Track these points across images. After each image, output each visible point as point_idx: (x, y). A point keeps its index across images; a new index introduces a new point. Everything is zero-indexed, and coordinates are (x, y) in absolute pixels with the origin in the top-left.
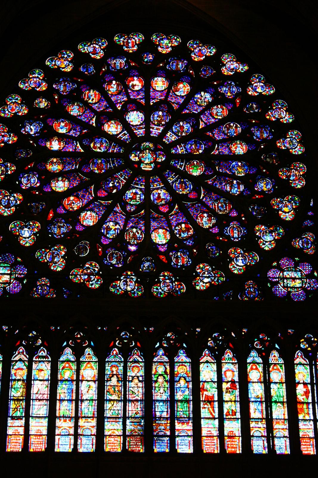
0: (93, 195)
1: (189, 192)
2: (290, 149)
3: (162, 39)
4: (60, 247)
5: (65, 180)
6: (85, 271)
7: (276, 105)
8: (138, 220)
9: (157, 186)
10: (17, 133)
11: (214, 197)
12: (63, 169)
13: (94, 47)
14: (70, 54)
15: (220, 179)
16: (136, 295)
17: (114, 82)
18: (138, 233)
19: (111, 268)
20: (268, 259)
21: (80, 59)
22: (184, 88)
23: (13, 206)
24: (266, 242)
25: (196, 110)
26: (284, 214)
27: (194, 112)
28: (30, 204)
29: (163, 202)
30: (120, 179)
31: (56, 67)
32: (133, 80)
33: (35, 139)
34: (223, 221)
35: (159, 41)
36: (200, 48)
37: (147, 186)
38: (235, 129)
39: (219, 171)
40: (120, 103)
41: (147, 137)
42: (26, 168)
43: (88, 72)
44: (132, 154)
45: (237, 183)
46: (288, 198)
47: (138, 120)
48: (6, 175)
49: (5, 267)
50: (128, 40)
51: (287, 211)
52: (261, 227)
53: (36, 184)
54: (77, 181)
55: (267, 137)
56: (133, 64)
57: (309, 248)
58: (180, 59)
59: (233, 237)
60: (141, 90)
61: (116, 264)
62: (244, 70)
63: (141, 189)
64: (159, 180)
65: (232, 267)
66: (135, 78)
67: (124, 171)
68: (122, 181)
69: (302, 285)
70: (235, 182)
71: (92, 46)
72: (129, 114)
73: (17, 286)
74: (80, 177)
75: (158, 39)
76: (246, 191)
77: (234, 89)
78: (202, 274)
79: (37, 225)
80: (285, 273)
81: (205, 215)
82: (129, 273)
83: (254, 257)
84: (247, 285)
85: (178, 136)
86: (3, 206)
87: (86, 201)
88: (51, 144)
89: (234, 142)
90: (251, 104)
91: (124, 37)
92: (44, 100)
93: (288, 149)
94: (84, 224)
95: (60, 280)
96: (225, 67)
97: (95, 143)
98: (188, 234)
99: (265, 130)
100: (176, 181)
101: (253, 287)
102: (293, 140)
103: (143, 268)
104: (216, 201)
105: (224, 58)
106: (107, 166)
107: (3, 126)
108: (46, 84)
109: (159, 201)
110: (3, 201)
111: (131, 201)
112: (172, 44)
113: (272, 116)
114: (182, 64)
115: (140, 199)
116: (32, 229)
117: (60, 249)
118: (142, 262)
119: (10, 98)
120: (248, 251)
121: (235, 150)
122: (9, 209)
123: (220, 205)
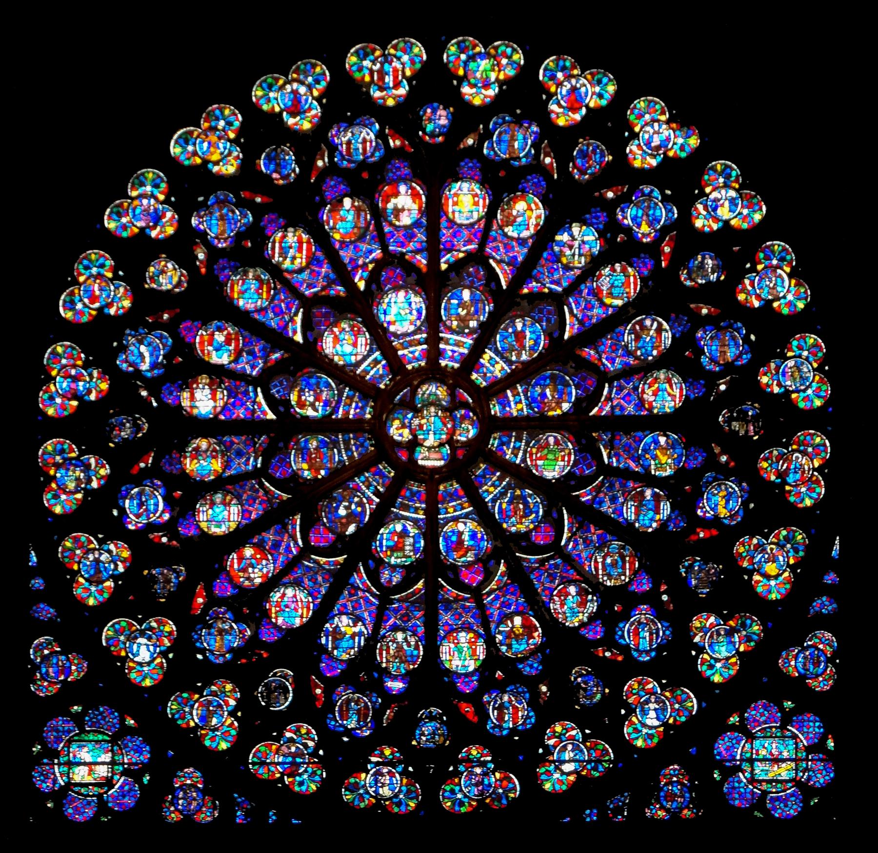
0: (300, 542)
1: (535, 528)
2: (793, 392)
3: (472, 58)
4: (224, 687)
5: (231, 500)
6: (284, 749)
7: (768, 258)
8: (407, 608)
9: (455, 511)
10: (110, 370)
11: (595, 538)
12: (224, 471)
13: (295, 92)
14: (232, 118)
15: (611, 487)
16: (403, 808)
17: (347, 202)
18: (409, 645)
19: (345, 739)
20: (721, 706)
21: (260, 132)
22: (528, 213)
23: (108, 580)
24: (717, 660)
25: (558, 283)
26: (765, 581)
27: (553, 286)
28: (149, 571)
29: (470, 557)
30: (363, 494)
31: (198, 161)
32: (397, 194)
33: (154, 386)
34: (614, 604)
35: (466, 63)
36: (573, 81)
37: (432, 512)
38: (658, 334)
39: (610, 464)
40: (364, 266)
41: (432, 371)
42: (134, 471)
43: (279, 173)
44: (394, 419)
45: (655, 496)
46: (777, 536)
47: (410, 317)
48: (88, 492)
49: (97, 742)
50: (382, 64)
51: (773, 573)
52: (707, 620)
53: (160, 516)
54: (260, 504)
55: (739, 357)
56: (398, 143)
57: (821, 675)
58: (518, 121)
59: (637, 650)
60: (417, 224)
61: (357, 729)
62: (687, 149)
63: (415, 522)
64: (462, 493)
65: (630, 730)
66: (402, 188)
67: (373, 469)
68: (370, 501)
69: (796, 774)
70: (648, 493)
71: (288, 87)
72: (387, 300)
73: (130, 790)
74: (267, 492)
75: (463, 57)
76: (676, 518)
77: (658, 213)
78: (558, 753)
79: (167, 629)
80: (757, 743)
81: (572, 590)
82: (387, 752)
83: (685, 701)
84: (665, 775)
85: (509, 362)
86: (86, 580)
87: (282, 559)
88: (192, 398)
89: (652, 376)
90: (699, 256)
91: (373, 54)
92: (170, 266)
93: (788, 393)
94: (280, 621)
95: (227, 774)
96: (636, 142)
97: (301, 392)
98: (528, 644)
99: (733, 338)
100: (503, 494)
101: (679, 782)
102: (802, 364)
103: (420, 738)
104: (599, 549)
105: (636, 111)
106: (332, 457)
107: (74, 349)
108: (173, 217)
109: (461, 553)
110: (85, 565)
111: (390, 557)
112: (499, 71)
113: (751, 293)
114: (525, 138)
115: (416, 550)
116: (158, 640)
117: (225, 692)
118: (417, 723)
119: (85, 262)
120: (672, 685)
121: (652, 399)
122: (100, 587)
123: (609, 560)
